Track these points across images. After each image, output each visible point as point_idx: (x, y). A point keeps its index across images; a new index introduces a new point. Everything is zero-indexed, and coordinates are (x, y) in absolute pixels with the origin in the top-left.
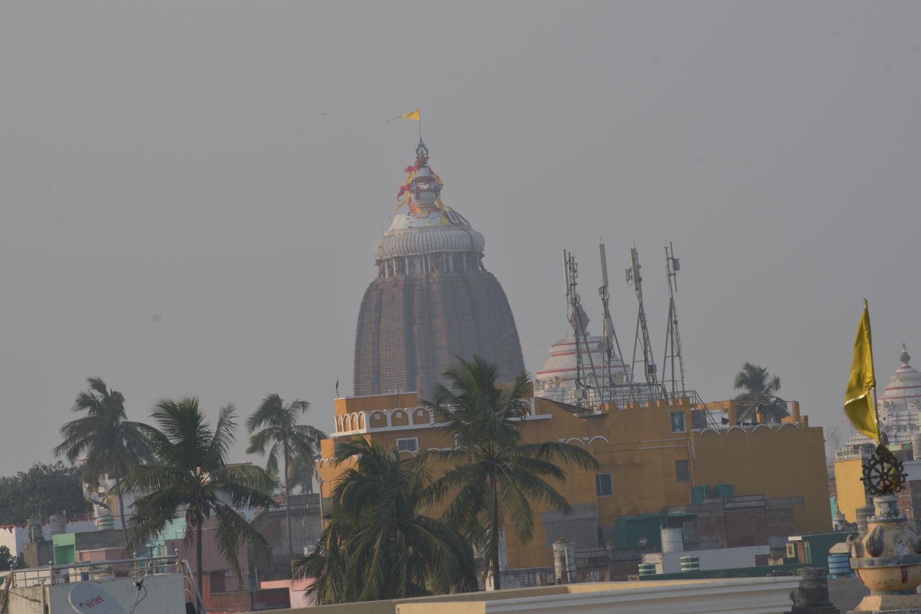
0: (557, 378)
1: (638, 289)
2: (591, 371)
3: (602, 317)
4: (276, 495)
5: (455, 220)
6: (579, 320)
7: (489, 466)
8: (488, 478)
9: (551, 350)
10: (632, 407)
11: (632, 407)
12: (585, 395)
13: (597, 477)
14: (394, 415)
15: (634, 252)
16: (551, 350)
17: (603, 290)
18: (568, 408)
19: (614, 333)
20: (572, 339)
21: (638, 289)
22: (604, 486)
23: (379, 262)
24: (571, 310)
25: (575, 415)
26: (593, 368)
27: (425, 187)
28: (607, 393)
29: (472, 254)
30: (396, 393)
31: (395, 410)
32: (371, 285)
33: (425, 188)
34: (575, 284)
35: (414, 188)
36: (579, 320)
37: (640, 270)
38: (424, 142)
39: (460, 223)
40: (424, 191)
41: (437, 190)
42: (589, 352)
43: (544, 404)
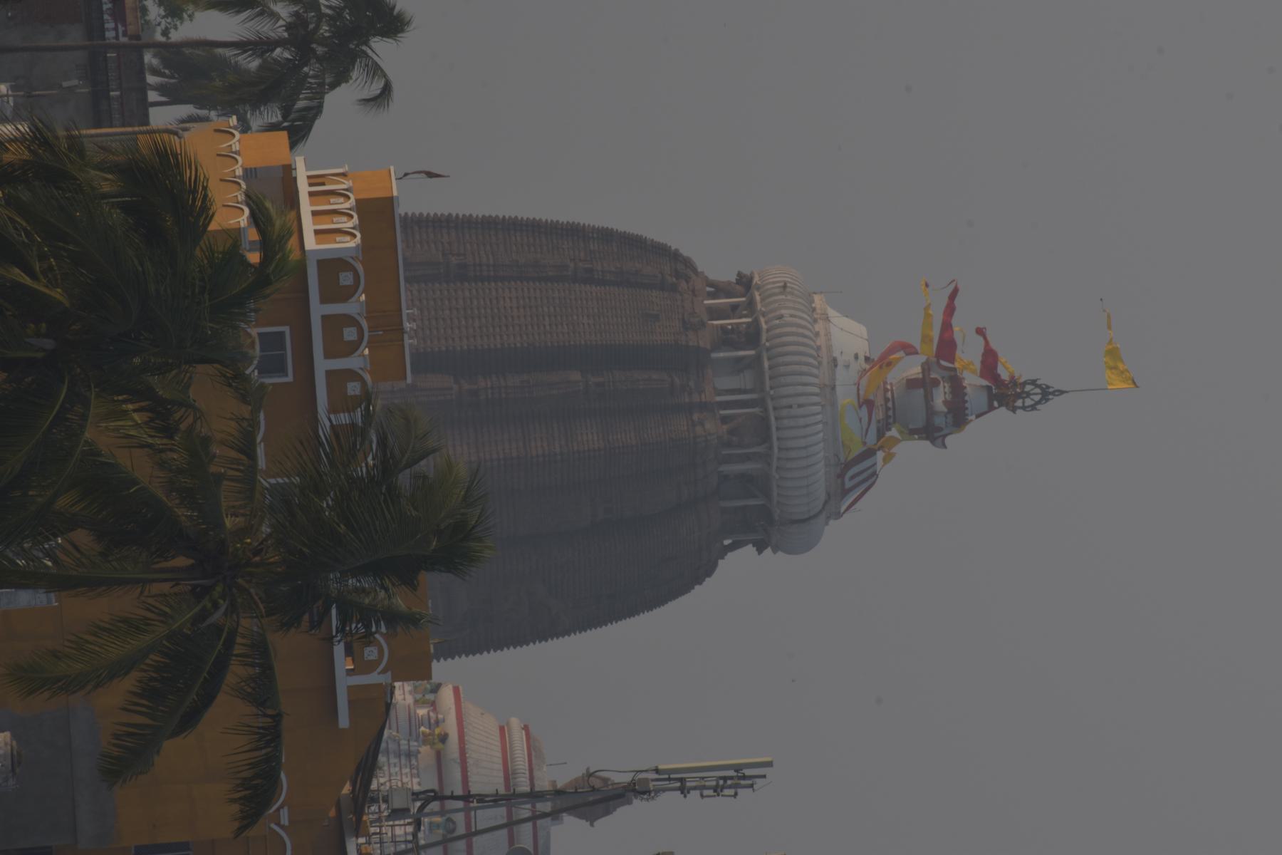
0: (444, 738)
2: (461, 830)
5: (852, 475)
9: (515, 723)
12: (397, 813)
14: (350, 320)
16: (515, 723)
18: (367, 767)
20: (543, 784)
23: (745, 283)
25: (347, 789)
26: (469, 835)
30: (407, 325)
32: (688, 263)
34: (684, 790)
38: (1055, 402)
39: (845, 492)
40: (928, 398)
41: (931, 433)
42: (511, 824)
43: (375, 707)
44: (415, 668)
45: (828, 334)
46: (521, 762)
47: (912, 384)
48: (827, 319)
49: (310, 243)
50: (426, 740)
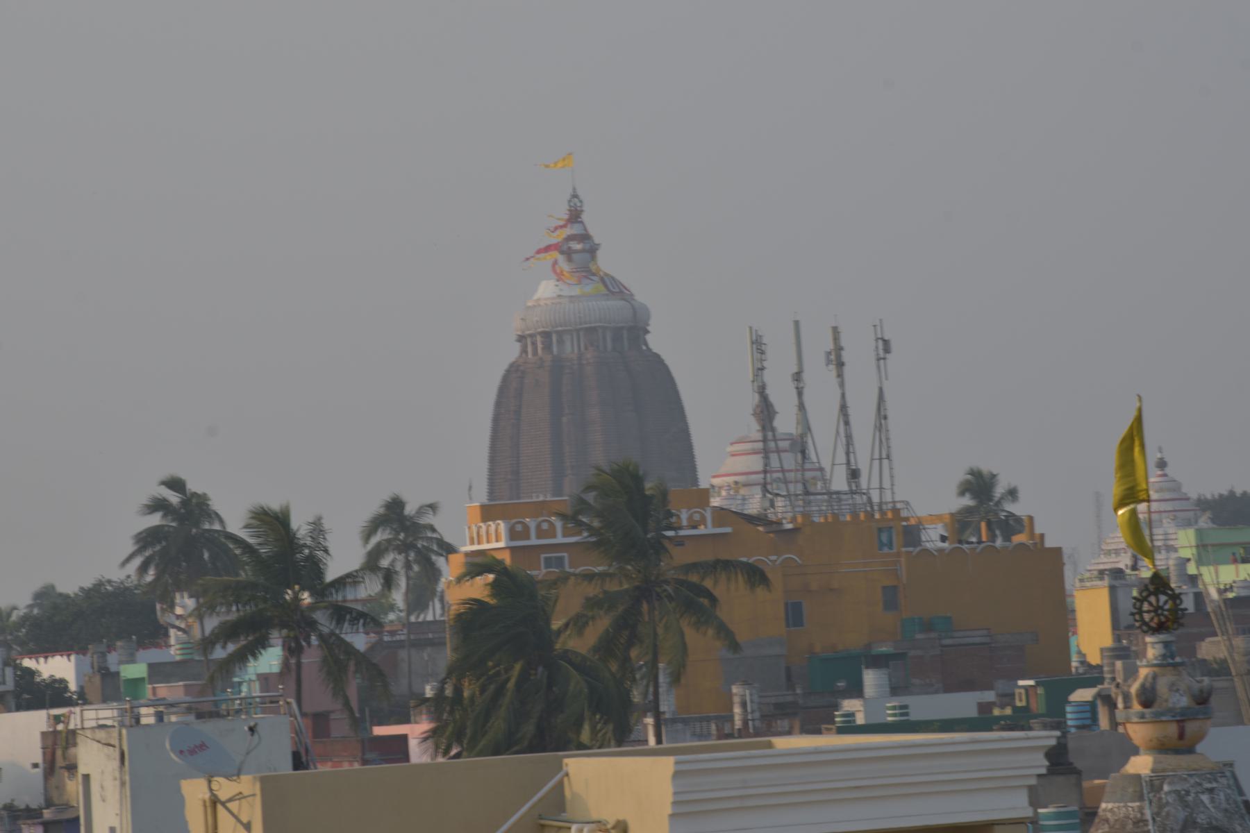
0: (736, 483)
1: (840, 375)
2: (780, 475)
3: (795, 410)
4: (392, 622)
5: (614, 288)
6: (765, 412)
7: (646, 591)
8: (645, 606)
9: (730, 449)
10: (830, 520)
11: (830, 520)
12: (772, 505)
13: (786, 604)
14: (538, 526)
15: (836, 331)
16: (730, 449)
17: (798, 377)
18: (750, 519)
19: (809, 429)
20: (759, 436)
21: (840, 375)
22: (794, 615)
23: (521, 338)
24: (757, 397)
25: (761, 529)
26: (783, 471)
27: (577, 246)
28: (801, 503)
29: (634, 330)
30: (541, 499)
31: (540, 519)
32: (512, 365)
33: (577, 248)
34: (762, 369)
35: (565, 248)
36: (765, 412)
37: (844, 353)
38: (580, 192)
39: (621, 292)
40: (577, 252)
41: (592, 251)
42: (778, 451)
43: (722, 515)
44: (704, 495)
45: (546, 299)
46: (748, 446)
47: (570, 260)
48: (539, 300)
49: (502, 544)
50: (737, 492)
